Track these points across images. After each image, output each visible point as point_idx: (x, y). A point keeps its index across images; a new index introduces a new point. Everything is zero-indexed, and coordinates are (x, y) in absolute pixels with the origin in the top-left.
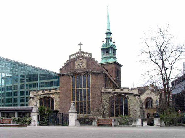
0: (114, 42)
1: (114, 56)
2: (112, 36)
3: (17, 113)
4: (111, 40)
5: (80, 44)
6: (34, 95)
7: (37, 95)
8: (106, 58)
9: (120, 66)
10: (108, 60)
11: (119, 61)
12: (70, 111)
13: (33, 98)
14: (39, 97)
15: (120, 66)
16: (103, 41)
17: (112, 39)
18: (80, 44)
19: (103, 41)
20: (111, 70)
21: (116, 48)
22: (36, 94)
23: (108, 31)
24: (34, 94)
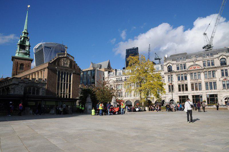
6: (19, 82)
7: (22, 82)
10: (25, 56)
14: (24, 85)
20: (27, 65)
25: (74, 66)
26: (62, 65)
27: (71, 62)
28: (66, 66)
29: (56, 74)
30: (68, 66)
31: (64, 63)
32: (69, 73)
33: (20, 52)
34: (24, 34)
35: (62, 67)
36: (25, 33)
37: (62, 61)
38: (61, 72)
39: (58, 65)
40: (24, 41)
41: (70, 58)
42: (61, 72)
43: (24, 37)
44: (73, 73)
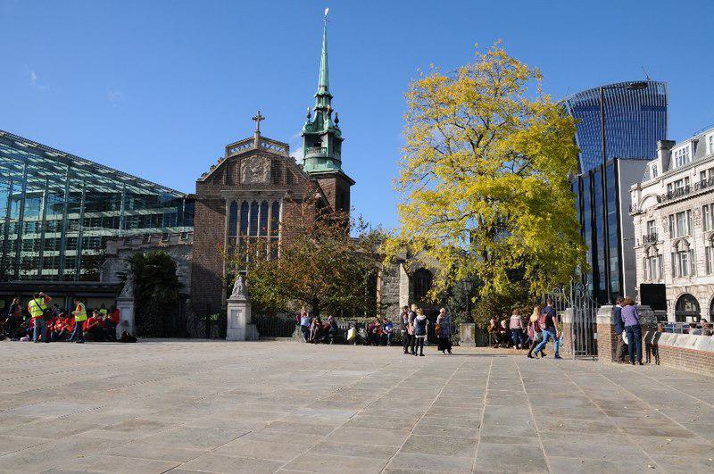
0: (337, 121)
1: (336, 157)
2: (334, 105)
3: (71, 298)
4: (329, 115)
5: (259, 119)
6: (119, 251)
8: (312, 160)
9: (351, 182)
11: (347, 169)
12: (233, 297)
13: (115, 256)
15: (351, 182)
16: (309, 116)
17: (331, 111)
18: (259, 119)
19: (309, 116)
21: (342, 137)
22: (126, 247)
23: (321, 91)
24: (120, 248)
25: (289, 174)
26: (243, 180)
27: (276, 162)
28: (255, 180)
29: (223, 212)
30: (264, 178)
31: (249, 173)
32: (270, 203)
33: (308, 156)
34: (319, 102)
35: (243, 185)
36: (320, 97)
37: (242, 165)
38: (239, 203)
39: (229, 182)
40: (320, 120)
41: (273, 149)
42: (239, 203)
43: (318, 109)
44: (287, 200)
